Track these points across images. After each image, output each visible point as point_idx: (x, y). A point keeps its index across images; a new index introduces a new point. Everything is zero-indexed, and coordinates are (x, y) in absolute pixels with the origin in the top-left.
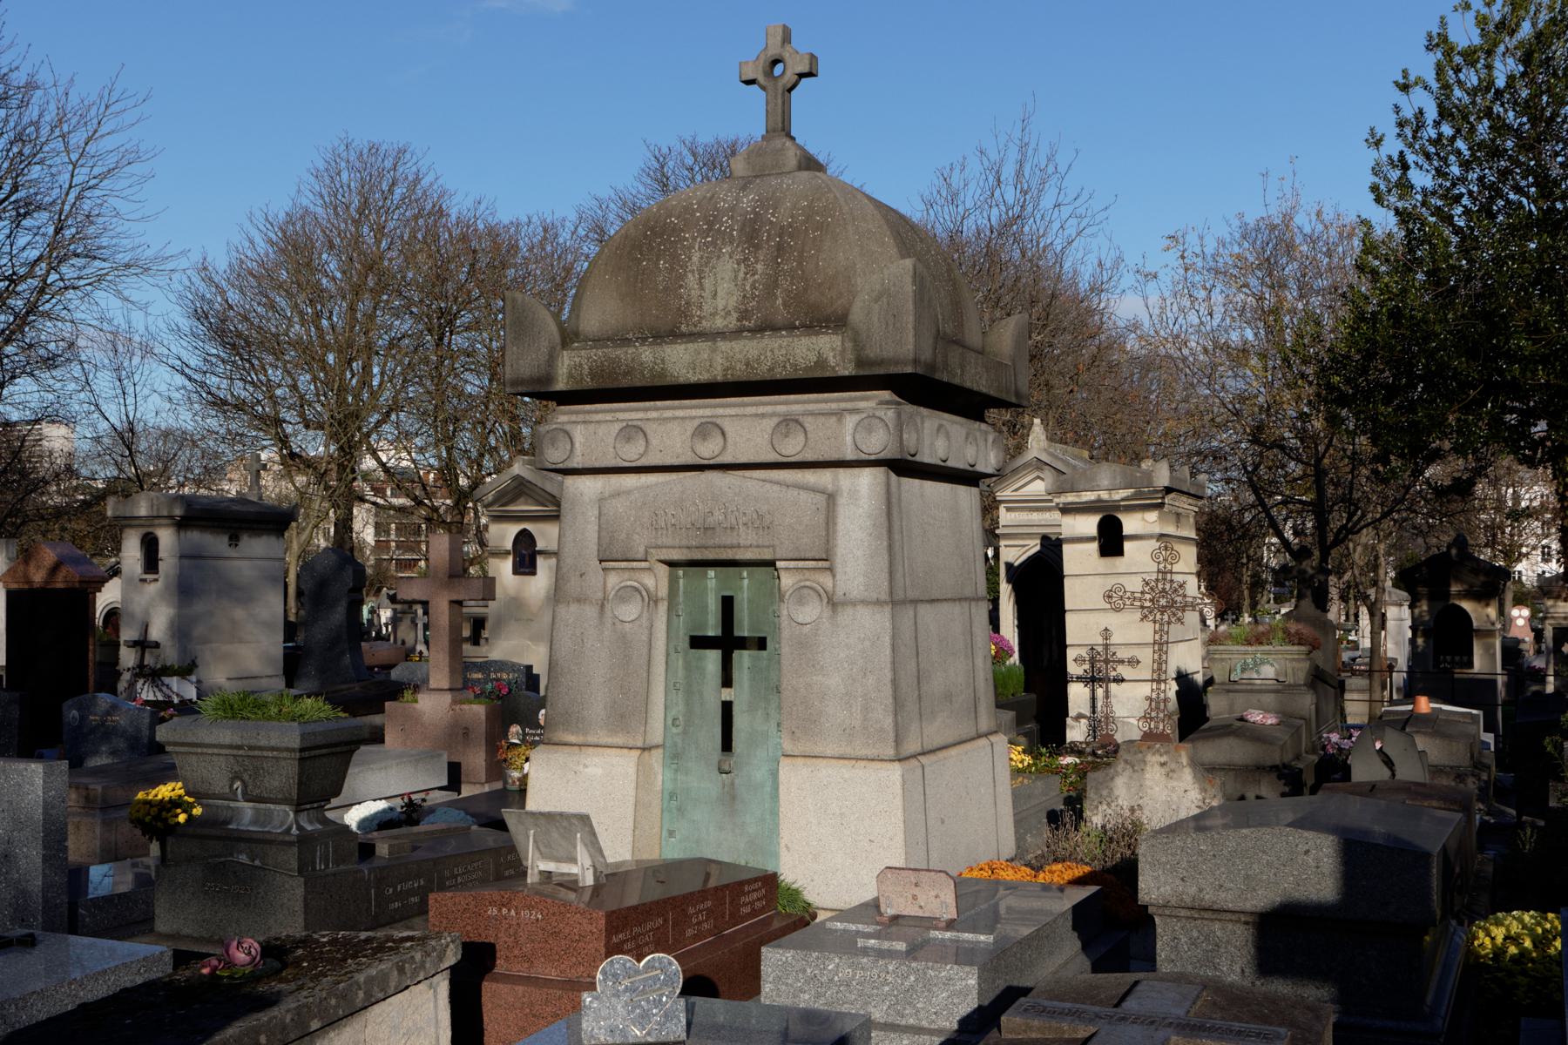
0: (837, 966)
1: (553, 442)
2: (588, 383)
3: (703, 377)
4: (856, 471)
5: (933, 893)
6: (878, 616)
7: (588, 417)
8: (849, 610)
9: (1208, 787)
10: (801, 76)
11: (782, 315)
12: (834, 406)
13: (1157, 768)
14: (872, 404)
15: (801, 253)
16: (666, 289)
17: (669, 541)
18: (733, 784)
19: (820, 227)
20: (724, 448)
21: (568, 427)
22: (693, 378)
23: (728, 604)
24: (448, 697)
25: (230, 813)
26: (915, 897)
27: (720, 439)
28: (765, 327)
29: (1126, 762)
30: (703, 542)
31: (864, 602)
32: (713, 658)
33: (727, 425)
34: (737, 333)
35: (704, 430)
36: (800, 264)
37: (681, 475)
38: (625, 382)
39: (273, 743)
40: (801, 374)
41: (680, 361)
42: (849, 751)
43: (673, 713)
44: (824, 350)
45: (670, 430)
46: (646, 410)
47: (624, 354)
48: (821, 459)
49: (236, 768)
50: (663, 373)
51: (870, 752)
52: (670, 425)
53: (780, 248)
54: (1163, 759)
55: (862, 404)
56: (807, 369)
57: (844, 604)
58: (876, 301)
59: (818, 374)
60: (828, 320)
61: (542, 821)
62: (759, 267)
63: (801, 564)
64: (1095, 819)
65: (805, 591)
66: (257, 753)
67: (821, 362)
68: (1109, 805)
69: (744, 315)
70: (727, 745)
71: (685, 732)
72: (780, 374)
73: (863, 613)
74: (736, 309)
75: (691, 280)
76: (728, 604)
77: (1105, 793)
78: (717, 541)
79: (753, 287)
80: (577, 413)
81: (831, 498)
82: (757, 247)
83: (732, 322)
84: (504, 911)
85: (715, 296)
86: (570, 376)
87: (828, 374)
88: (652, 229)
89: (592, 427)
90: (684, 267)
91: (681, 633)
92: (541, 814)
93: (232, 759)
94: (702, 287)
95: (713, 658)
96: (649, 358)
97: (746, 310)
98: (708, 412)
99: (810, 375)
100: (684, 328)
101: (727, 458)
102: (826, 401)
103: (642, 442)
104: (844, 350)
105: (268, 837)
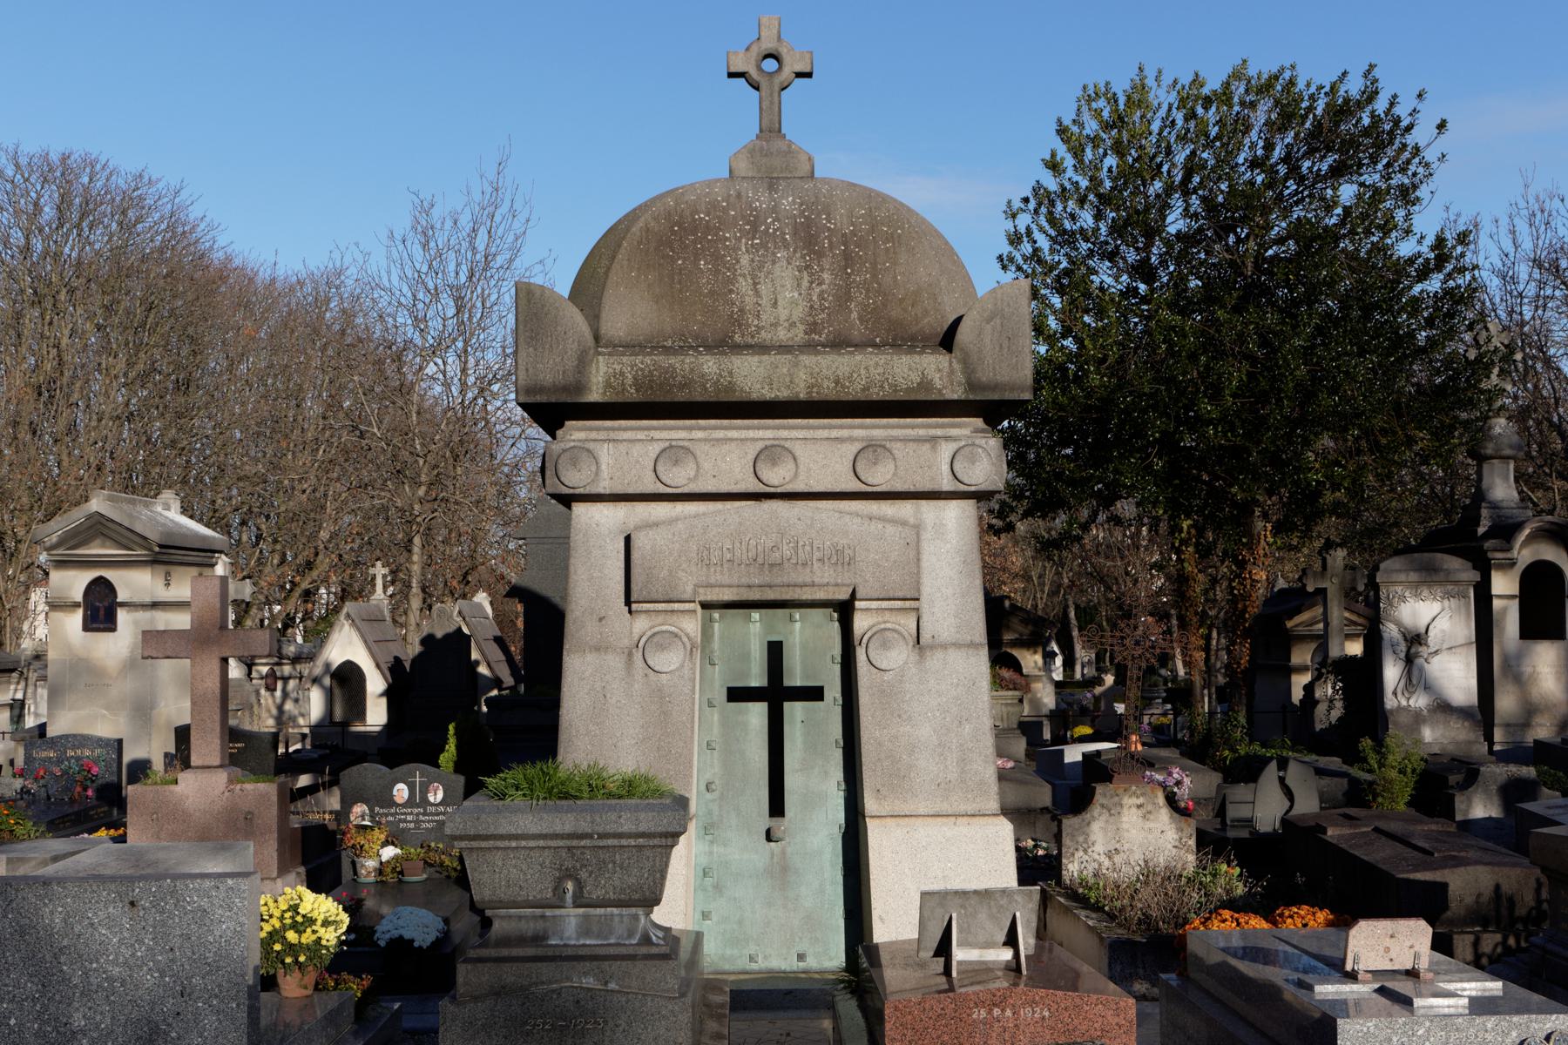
0: (1428, 1030)
1: (574, 462)
2: (632, 395)
3: (784, 394)
4: (941, 503)
5: (1408, 944)
6: (973, 660)
7: (612, 435)
8: (939, 654)
9: (1183, 825)
10: (799, 75)
11: (858, 331)
12: (922, 432)
13: (1134, 810)
14: (966, 432)
15: (874, 264)
16: (712, 293)
17: (726, 580)
18: (783, 853)
19: (890, 238)
20: (796, 475)
21: (591, 446)
22: (769, 394)
23: (775, 652)
24: (221, 777)
25: (540, 925)
26: (1387, 950)
27: (791, 465)
28: (838, 344)
29: (1102, 806)
30: (767, 579)
31: (957, 645)
32: (757, 713)
33: (798, 448)
34: (810, 347)
35: (770, 454)
36: (874, 276)
37: (729, 505)
38: (681, 396)
39: (643, 828)
40: (901, 396)
41: (752, 375)
42: (945, 807)
43: (708, 776)
44: (934, 372)
45: (724, 452)
46: (691, 429)
47: (681, 364)
48: (912, 489)
49: (568, 864)
50: (731, 387)
51: (970, 808)
52: (726, 447)
53: (847, 258)
54: (1139, 801)
55: (954, 432)
56: (909, 390)
57: (932, 647)
58: (989, 320)
59: (922, 397)
60: (913, 338)
61: (974, 901)
62: (825, 276)
63: (885, 604)
64: (1070, 867)
65: (888, 634)
66: (610, 842)
67: (925, 384)
68: (1085, 851)
69: (813, 328)
70: (777, 807)
71: (722, 797)
72: (876, 394)
73: (956, 658)
74: (802, 321)
75: (744, 285)
76: (775, 652)
77: (1081, 839)
78: (785, 580)
79: (821, 296)
80: (598, 429)
81: (918, 528)
82: (820, 255)
83: (799, 334)
84: (997, 1012)
85: (775, 305)
86: (608, 385)
87: (933, 397)
88: (679, 224)
89: (623, 447)
90: (732, 268)
91: (717, 684)
92: (975, 892)
93: (563, 853)
94: (757, 293)
95: (757, 713)
96: (710, 370)
97: (815, 323)
98: (769, 434)
99: (913, 397)
100: (737, 338)
101: (800, 487)
102: (913, 427)
103: (692, 465)
104: (952, 372)
105: (581, 952)
